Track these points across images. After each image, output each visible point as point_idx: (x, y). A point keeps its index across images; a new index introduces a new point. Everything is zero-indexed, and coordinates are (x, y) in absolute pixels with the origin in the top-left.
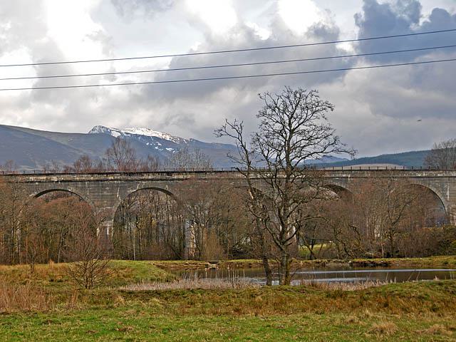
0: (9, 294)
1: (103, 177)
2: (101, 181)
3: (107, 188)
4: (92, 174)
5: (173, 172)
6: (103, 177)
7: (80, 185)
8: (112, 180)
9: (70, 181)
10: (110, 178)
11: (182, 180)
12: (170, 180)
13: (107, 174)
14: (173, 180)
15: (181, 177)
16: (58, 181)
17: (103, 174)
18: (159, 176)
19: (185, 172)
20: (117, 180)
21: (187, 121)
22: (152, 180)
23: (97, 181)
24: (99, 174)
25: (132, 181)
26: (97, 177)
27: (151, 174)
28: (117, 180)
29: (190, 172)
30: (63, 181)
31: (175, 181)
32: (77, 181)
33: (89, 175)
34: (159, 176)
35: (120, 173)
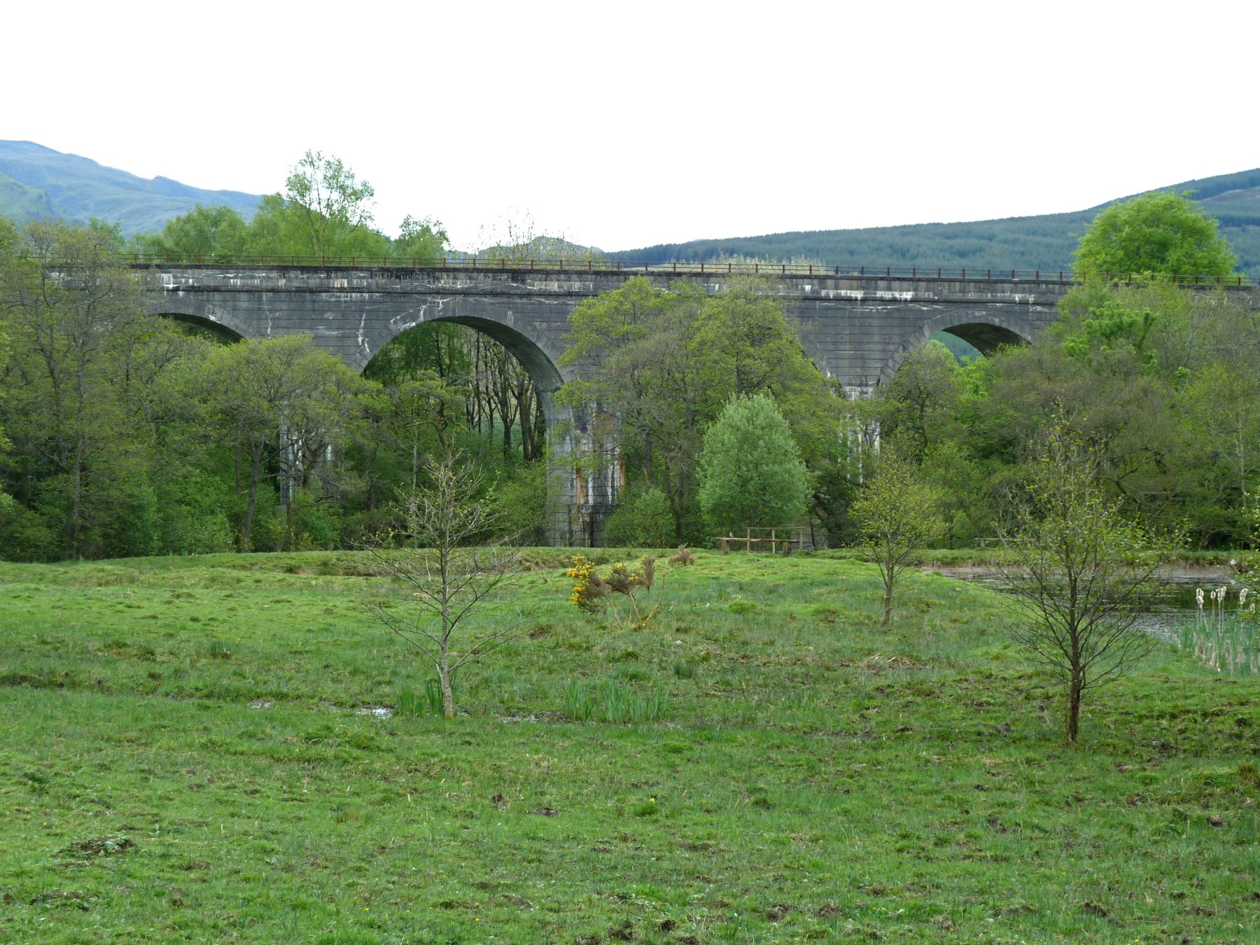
0: (996, 859)
1: (314, 281)
2: (312, 291)
3: (330, 316)
4: (284, 269)
5: (531, 272)
6: (314, 281)
7: (244, 302)
8: (342, 290)
9: (217, 290)
10: (337, 284)
11: (556, 295)
12: (522, 296)
13: (328, 270)
14: (529, 295)
15: (554, 286)
16: (176, 290)
17: (316, 270)
18: (485, 283)
19: (566, 272)
20: (360, 290)
21: (975, 317)
22: (465, 293)
23: (300, 291)
24: (304, 269)
25: (404, 294)
26: (298, 280)
27: (462, 275)
28: (360, 290)
29: (580, 273)
30: (189, 289)
31: (535, 299)
32: (236, 291)
33: (274, 274)
34: (485, 283)
35: (368, 270)
